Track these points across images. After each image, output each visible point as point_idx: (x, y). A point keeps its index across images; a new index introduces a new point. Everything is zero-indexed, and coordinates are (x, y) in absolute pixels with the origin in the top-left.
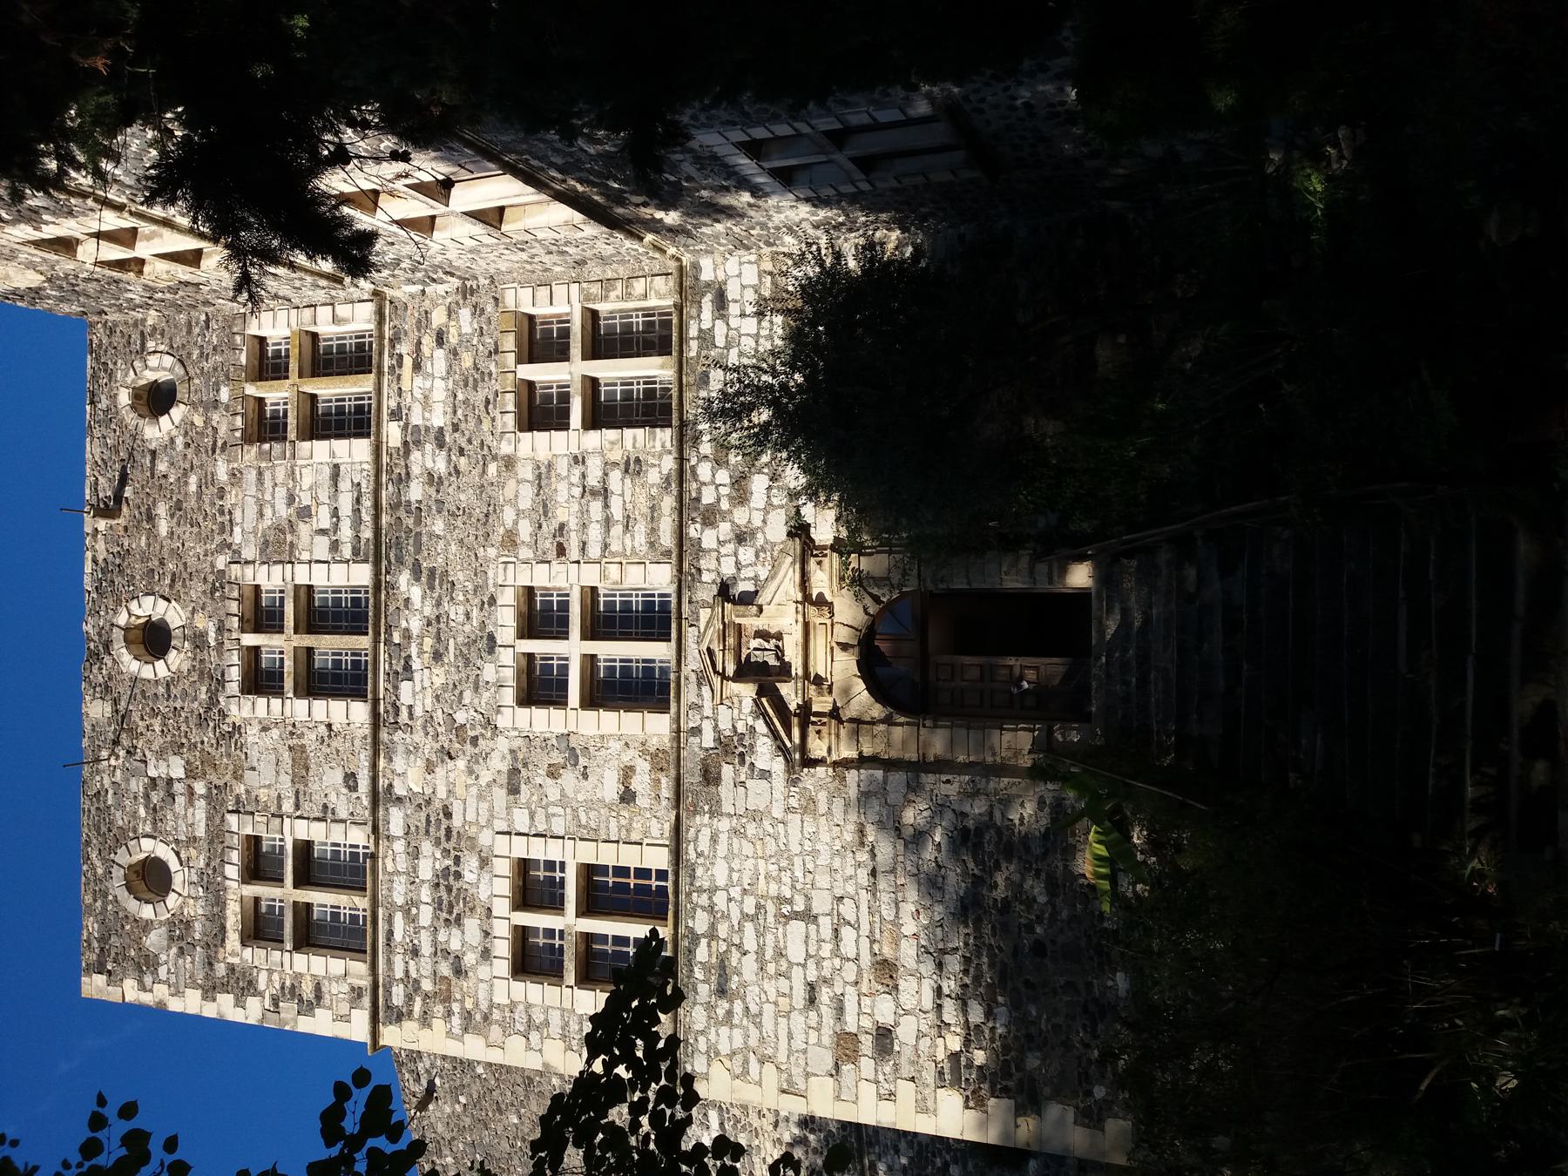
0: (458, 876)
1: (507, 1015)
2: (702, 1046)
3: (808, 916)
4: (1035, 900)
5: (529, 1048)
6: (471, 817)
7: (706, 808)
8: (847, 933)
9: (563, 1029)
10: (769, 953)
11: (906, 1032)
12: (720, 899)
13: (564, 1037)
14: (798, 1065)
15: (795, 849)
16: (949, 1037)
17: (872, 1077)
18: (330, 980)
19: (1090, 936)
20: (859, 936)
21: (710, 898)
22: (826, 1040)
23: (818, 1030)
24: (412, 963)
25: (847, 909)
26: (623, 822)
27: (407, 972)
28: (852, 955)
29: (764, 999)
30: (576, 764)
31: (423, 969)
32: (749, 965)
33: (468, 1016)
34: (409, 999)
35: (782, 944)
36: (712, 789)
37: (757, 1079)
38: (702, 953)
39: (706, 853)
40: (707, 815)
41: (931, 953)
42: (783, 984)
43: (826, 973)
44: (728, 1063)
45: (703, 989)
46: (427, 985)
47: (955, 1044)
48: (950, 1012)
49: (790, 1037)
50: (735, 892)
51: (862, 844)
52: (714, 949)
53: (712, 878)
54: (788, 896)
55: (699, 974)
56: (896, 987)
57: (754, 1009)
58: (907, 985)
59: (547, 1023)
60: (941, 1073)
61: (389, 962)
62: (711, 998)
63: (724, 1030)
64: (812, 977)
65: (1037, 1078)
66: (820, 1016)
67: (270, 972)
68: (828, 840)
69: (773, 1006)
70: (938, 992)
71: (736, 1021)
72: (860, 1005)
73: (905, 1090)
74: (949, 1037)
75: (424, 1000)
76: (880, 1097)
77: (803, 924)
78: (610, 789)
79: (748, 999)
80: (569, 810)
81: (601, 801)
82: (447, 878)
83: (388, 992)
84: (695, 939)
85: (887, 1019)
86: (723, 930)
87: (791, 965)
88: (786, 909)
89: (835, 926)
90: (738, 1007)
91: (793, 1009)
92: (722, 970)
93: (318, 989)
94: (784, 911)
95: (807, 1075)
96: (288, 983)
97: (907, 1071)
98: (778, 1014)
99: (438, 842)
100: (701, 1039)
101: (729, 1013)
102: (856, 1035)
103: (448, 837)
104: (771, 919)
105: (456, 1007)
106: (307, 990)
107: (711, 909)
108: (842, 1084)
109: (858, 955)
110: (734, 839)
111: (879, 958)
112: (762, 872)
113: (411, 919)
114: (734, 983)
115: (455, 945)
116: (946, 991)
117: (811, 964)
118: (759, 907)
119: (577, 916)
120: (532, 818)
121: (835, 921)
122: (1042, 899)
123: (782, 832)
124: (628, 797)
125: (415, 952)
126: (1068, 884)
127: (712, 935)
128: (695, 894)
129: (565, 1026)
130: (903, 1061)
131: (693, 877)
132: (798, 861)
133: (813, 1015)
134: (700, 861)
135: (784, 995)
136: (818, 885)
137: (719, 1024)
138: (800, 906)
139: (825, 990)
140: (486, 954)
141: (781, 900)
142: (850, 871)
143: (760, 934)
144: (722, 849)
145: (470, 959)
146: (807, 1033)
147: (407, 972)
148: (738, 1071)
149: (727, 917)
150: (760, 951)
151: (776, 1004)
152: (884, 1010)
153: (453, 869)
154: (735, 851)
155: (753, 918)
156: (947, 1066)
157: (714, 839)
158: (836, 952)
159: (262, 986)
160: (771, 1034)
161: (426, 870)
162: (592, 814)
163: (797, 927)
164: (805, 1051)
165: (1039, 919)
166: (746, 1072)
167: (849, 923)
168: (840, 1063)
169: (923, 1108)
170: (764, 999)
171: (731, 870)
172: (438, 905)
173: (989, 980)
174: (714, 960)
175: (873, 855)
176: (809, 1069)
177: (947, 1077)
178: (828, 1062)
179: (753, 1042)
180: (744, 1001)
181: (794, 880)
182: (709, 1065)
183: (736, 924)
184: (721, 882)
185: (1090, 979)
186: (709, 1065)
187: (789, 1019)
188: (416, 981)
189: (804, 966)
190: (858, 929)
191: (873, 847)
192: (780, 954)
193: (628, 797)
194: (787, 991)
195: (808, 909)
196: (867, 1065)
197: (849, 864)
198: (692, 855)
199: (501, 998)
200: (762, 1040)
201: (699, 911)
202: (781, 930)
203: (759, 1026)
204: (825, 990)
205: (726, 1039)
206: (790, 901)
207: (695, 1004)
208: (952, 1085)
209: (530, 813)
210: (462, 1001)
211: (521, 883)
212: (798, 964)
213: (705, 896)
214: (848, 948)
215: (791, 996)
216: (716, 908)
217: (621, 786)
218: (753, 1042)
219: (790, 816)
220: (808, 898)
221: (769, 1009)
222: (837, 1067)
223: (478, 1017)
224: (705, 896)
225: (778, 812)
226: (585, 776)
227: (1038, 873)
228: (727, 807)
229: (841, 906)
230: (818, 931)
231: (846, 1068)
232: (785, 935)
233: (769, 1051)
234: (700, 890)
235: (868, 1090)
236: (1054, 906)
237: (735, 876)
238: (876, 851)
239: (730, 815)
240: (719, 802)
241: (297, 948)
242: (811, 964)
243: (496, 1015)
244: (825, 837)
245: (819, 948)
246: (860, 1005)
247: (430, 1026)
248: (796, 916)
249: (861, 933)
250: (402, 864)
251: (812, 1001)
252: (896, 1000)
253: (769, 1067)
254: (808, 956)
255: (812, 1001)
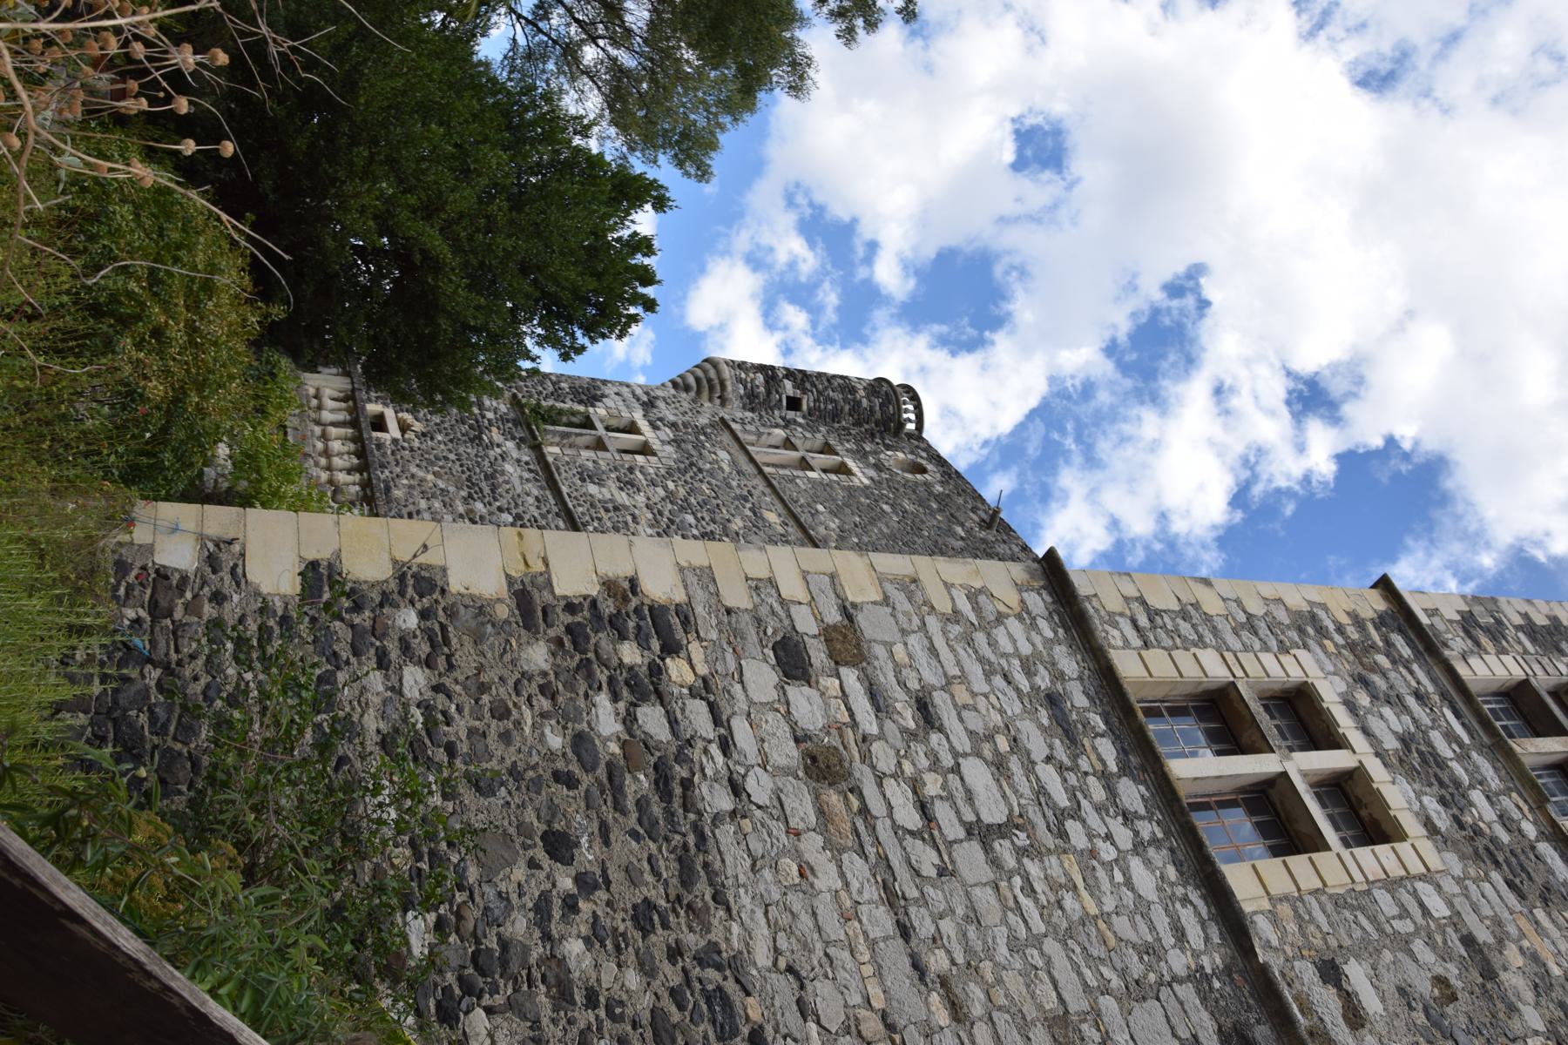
0: (1443, 801)
1: (1282, 637)
2: (1043, 624)
3: (981, 833)
4: (587, 941)
5: (1238, 602)
6: (1487, 886)
7: (1217, 984)
8: (910, 818)
9: (1215, 628)
10: (1015, 765)
11: (762, 677)
12: (1124, 837)
13: (1208, 618)
14: (905, 613)
15: (1051, 946)
16: (690, 678)
17: (794, 609)
18: (1472, 652)
19: (460, 887)
20: (890, 815)
21: (1136, 833)
22: (879, 651)
23: (896, 665)
24: (1414, 684)
25: (927, 859)
26: (1312, 928)
27: (1411, 672)
28: (890, 786)
29: (993, 699)
30: (1426, 1009)
31: (1401, 681)
32: (1037, 746)
33: (1322, 632)
34: (1388, 643)
35: (1004, 784)
36: (1228, 1024)
37: (954, 591)
38: (1107, 750)
39: (1178, 905)
40: (1208, 970)
41: (759, 807)
42: (974, 722)
43: (919, 749)
44: (1002, 609)
45: (1081, 700)
46: (1382, 660)
47: (677, 670)
48: (698, 717)
49: (933, 651)
50: (1107, 852)
51: (944, 982)
52: (1094, 757)
53: (1148, 863)
54: (1025, 860)
55: (1098, 722)
56: (797, 740)
57: (998, 681)
58: (786, 753)
59: (1236, 632)
60: (686, 622)
61: (1433, 680)
62: (1064, 689)
63: (1026, 649)
64: (935, 738)
65: (523, 632)
66: (903, 684)
67: (1526, 652)
68: (1008, 977)
69: (975, 690)
70: (726, 745)
71: (1016, 662)
72: (849, 709)
73: (736, 596)
74: (690, 678)
75: (1374, 643)
76: (772, 582)
77: (987, 818)
78: (1356, 973)
79: (1012, 694)
80: (1389, 930)
81: (1358, 957)
82: (1453, 797)
83: (1410, 643)
84: (1125, 769)
85: (799, 695)
86: (1098, 792)
87: (979, 755)
88: (1022, 839)
89: (933, 825)
90: (1024, 684)
91: (947, 687)
92: (1066, 729)
93: (1477, 643)
94: (1023, 835)
95: (886, 601)
96: (1504, 643)
97: (745, 621)
98: (963, 678)
99: (1494, 840)
100: (1050, 634)
101: (1029, 673)
102: (837, 663)
103: (1487, 849)
104: (1034, 814)
105: (1339, 640)
106: (1485, 641)
107: (1128, 818)
108: (833, 596)
109: (880, 785)
110: (1150, 939)
111: (844, 786)
112: (1084, 894)
113: (1450, 736)
114: (1044, 716)
115: (1387, 711)
116: (714, 749)
117: (947, 761)
118: (1063, 835)
119: (1284, 775)
120: (1422, 905)
121: (936, 833)
122: (574, 947)
123: (1087, 973)
124: (1331, 972)
125: (1420, 696)
126: (525, 987)
127: (1105, 777)
128: (1160, 835)
129: (1215, 631)
130: (752, 636)
131: (1178, 865)
132: (1039, 926)
133: (914, 685)
134: (1180, 891)
135: (965, 707)
136: (989, 891)
137: (1036, 654)
138: (1003, 848)
139: (912, 725)
140: (1351, 706)
141: (1032, 851)
142: (947, 926)
143: (1041, 792)
144: (1162, 922)
145: (1363, 699)
146: (910, 656)
147: (1411, 672)
148: (982, 599)
149: (1098, 808)
150: (1029, 766)
151: (974, 695)
152: (807, 706)
153: (1455, 811)
154: (1138, 918)
155: (1062, 815)
156: (679, 633)
157: (1180, 934)
158: (916, 785)
159: (1521, 635)
160: (961, 652)
161: (1477, 796)
162: (1357, 933)
163: (994, 814)
164: (904, 632)
165: (570, 905)
166: (973, 596)
167: (911, 833)
168: (846, 622)
169: (707, 576)
170: (993, 699)
171: (1129, 883)
172: (1441, 763)
173: (642, 777)
174: (1086, 742)
175: (918, 967)
176: (889, 610)
177: (675, 621)
178: (861, 619)
179: (980, 638)
180: (1018, 690)
181: (1029, 889)
182: (1022, 601)
183: (1085, 803)
184: (1135, 864)
185: (450, 806)
186: (1022, 601)
187: (945, 675)
188: (1394, 662)
189: (956, 755)
190: (896, 827)
191: (922, 978)
192: (999, 766)
193: (1331, 972)
194: (965, 714)
195: (987, 848)
196: (806, 624)
197: (953, 937)
198: (1194, 896)
199: (1302, 654)
200: (970, 642)
201: (1142, 811)
202: (1015, 804)
203: (982, 660)
204: (912, 725)
205: (1014, 638)
206: (1021, 852)
207: (1080, 678)
208: (664, 609)
209: (1429, 913)
210: (1336, 645)
211: (1364, 813)
212: (965, 755)
213: (1146, 835)
214: (899, 795)
215: (955, 705)
216: (1120, 819)
217: (1350, 989)
218: (980, 638)
219: (1085, 1006)
220: (995, 863)
221: (980, 685)
222: (850, 618)
223: (1310, 631)
224: (1146, 835)
225: (1108, 1004)
226: (1402, 991)
227: (592, 1000)
228: (1187, 992)
229: (937, 861)
230: (958, 812)
231: (833, 616)
232: (1004, 796)
233: (956, 630)
234: (1154, 841)
235: (792, 587)
236: (547, 937)
237: (1119, 877)
238: (916, 975)
239: (1181, 981)
240: (1204, 1000)
241: (1524, 685)
242: (947, 761)
243: (1294, 635)
244: (1014, 982)
245: (944, 787)
246: (849, 709)
247: (1348, 613)
248: (1002, 831)
249: (888, 822)
250: (1506, 802)
251: (923, 706)
252: (793, 726)
253: (944, 606)
254: (956, 770)
255: (923, 706)
